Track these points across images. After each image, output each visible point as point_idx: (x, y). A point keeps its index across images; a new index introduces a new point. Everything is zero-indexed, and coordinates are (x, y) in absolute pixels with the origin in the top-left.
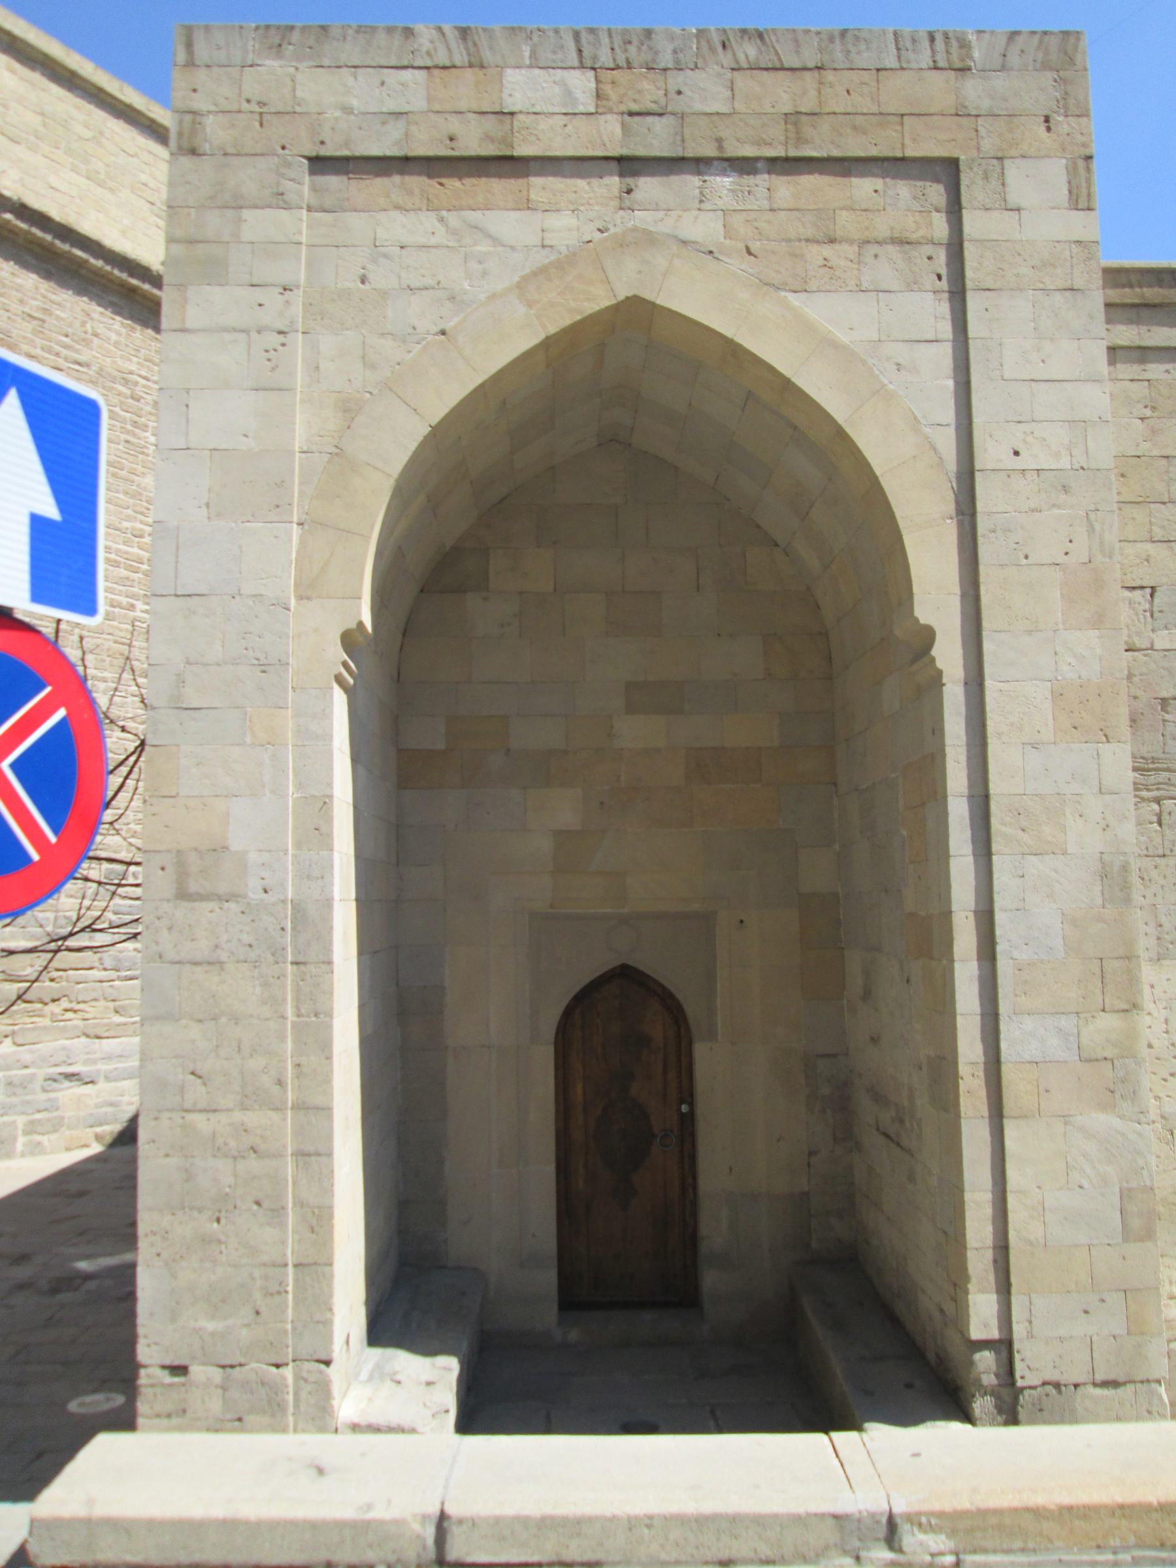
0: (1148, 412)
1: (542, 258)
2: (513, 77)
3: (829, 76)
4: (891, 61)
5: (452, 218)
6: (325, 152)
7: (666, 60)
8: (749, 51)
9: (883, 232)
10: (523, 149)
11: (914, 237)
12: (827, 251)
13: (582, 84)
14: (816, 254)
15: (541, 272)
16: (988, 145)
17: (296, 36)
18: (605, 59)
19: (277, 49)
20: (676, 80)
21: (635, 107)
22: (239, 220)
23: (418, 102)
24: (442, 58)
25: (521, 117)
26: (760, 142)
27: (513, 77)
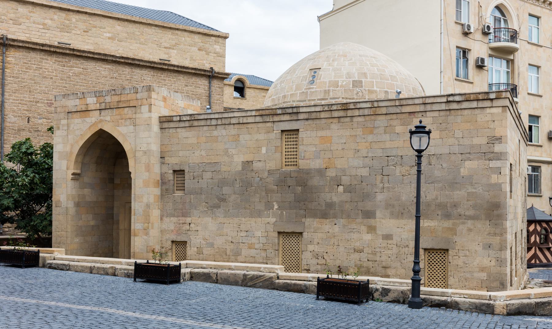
0: (169, 138)
1: (92, 124)
2: (88, 99)
3: (122, 95)
4: (129, 93)
5: (82, 119)
6: (69, 111)
7: (104, 95)
8: (113, 92)
9: (128, 117)
10: (89, 109)
11: (131, 118)
12: (121, 121)
13: (95, 99)
14: (120, 121)
15: (91, 126)
16: (139, 104)
17: (66, 95)
18: (98, 96)
19: (64, 98)
20: (106, 97)
21: (101, 102)
22: (61, 121)
23: (78, 104)
24: (81, 98)
25: (89, 105)
26: (114, 106)
27: (88, 99)
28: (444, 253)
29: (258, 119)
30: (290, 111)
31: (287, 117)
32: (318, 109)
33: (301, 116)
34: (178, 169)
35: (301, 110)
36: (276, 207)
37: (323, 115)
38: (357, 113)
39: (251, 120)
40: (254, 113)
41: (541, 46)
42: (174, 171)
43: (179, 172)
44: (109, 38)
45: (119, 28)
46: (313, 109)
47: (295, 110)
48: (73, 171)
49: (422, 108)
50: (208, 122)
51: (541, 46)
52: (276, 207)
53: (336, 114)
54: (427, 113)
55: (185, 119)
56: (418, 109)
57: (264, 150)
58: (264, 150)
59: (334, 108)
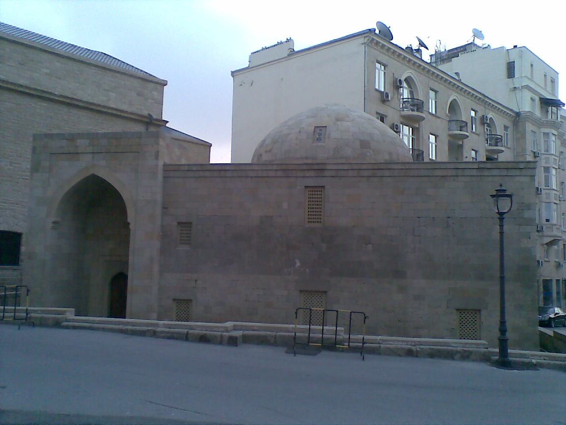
28: (476, 313)
29: (279, 173)
30: (316, 167)
31: (312, 173)
32: (346, 167)
33: (327, 173)
34: (185, 221)
35: (328, 167)
36: (298, 264)
37: (350, 173)
38: (387, 173)
39: (272, 174)
40: (275, 167)
41: (439, 118)
42: (179, 223)
43: (185, 225)
44: (46, 74)
45: (58, 64)
46: (340, 167)
47: (320, 167)
48: (54, 219)
49: (454, 173)
50: (223, 173)
51: (439, 118)
52: (298, 264)
53: (366, 173)
54: (459, 177)
55: (194, 169)
56: (450, 173)
57: (285, 205)
58: (285, 205)
59: (364, 167)
